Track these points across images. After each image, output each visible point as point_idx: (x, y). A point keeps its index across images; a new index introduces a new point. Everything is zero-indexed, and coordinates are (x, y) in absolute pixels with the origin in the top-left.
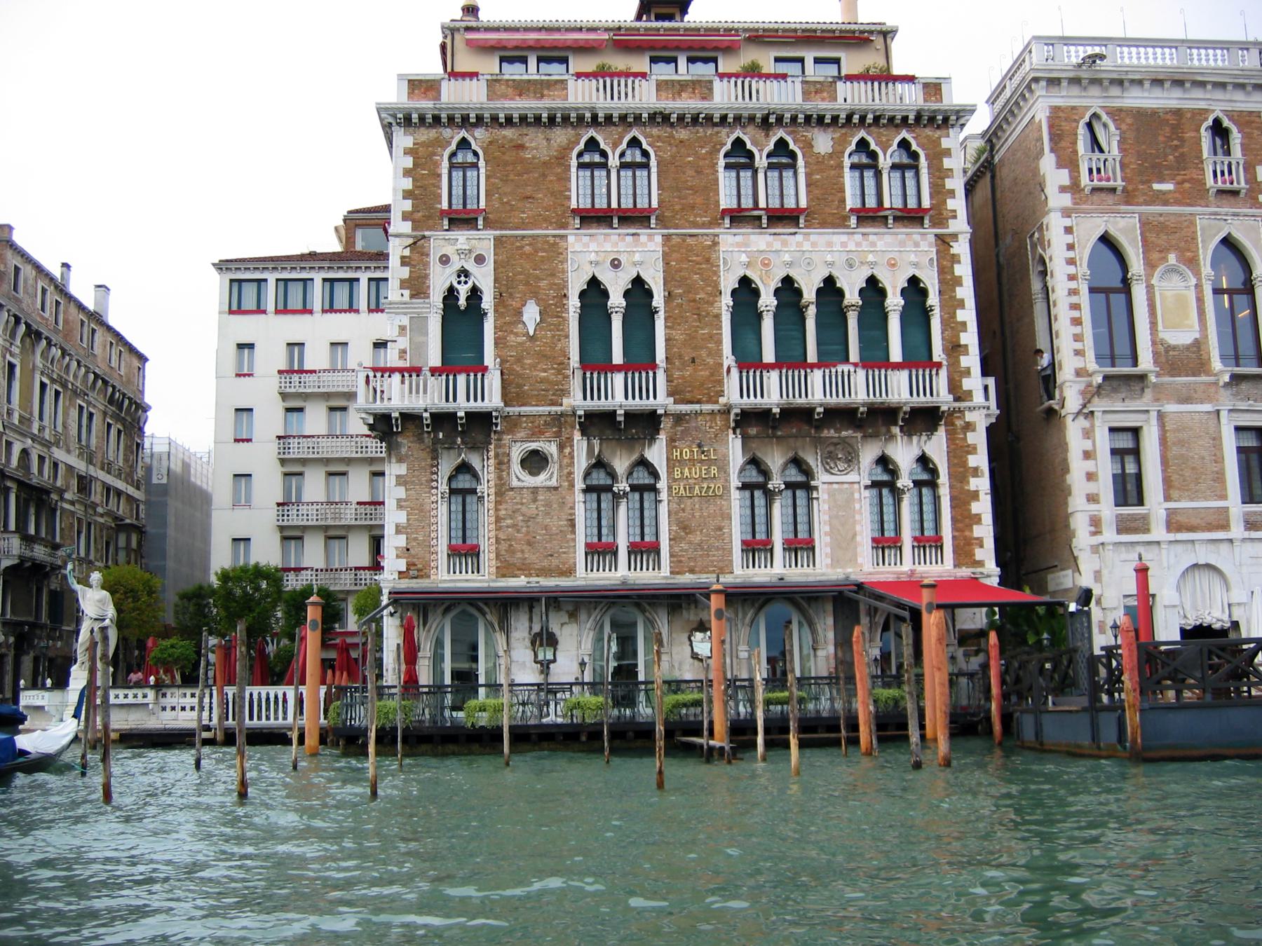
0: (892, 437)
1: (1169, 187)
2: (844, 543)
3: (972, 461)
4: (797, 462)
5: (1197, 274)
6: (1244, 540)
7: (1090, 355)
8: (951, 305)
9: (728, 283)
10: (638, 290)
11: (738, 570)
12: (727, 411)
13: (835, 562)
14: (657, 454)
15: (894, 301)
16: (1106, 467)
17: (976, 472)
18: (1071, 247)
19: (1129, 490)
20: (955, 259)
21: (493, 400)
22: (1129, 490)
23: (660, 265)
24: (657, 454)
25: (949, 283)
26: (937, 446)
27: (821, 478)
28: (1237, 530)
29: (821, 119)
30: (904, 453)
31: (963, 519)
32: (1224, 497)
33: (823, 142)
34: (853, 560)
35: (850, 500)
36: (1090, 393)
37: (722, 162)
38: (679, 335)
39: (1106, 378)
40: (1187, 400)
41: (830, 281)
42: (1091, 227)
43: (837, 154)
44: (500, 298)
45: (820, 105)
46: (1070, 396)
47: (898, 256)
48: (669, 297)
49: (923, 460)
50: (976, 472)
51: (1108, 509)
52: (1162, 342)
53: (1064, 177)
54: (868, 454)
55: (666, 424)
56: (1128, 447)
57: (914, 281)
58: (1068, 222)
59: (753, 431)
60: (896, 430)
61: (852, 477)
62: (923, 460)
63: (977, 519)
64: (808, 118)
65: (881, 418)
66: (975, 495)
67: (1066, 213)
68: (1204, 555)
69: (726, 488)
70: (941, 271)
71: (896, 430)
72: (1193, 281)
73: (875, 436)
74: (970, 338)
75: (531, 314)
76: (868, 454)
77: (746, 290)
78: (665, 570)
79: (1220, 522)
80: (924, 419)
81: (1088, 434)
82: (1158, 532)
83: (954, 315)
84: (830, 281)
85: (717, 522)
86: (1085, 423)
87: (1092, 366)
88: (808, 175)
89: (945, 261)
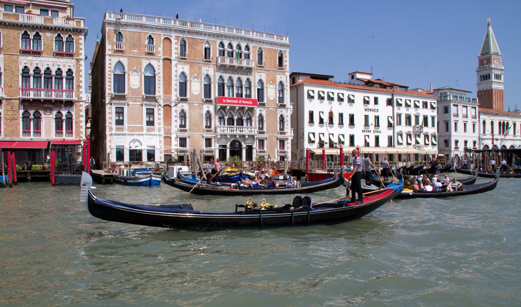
0: (61, 107)
1: (136, 51)
2: (48, 132)
3: (81, 113)
5: (141, 72)
6: (146, 134)
7: (112, 90)
9: (21, 67)
11: (21, 137)
12: (19, 99)
13: (46, 136)
17: (82, 116)
18: (110, 64)
19: (120, 122)
20: (81, 65)
22: (120, 122)
23: (3, 62)
25: (79, 71)
27: (43, 116)
28: (145, 132)
29: (48, 28)
32: (142, 124)
33: (48, 34)
34: (50, 136)
35: (50, 122)
36: (112, 99)
37: (21, 36)
38: (8, 80)
39: (115, 96)
40: (136, 101)
41: (48, 69)
42: (115, 60)
43: (52, 37)
45: (49, 24)
47: (65, 64)
48: (5, 70)
50: (82, 116)
51: (114, 126)
52: (131, 88)
55: (4, 101)
56: (120, 112)
57: (70, 70)
58: (110, 58)
59: (26, 104)
60: (63, 105)
61: (51, 116)
63: (81, 127)
64: (44, 28)
66: (81, 122)
67: (110, 55)
68: (136, 137)
69: (19, 117)
70: (77, 68)
71: (63, 105)
72: (140, 74)
73: (57, 107)
78: (3, 136)
79: (142, 129)
80: (70, 104)
81: (110, 108)
83: (79, 79)
84: (48, 69)
85: (16, 125)
86: (110, 106)
87: (113, 93)
88: (44, 42)
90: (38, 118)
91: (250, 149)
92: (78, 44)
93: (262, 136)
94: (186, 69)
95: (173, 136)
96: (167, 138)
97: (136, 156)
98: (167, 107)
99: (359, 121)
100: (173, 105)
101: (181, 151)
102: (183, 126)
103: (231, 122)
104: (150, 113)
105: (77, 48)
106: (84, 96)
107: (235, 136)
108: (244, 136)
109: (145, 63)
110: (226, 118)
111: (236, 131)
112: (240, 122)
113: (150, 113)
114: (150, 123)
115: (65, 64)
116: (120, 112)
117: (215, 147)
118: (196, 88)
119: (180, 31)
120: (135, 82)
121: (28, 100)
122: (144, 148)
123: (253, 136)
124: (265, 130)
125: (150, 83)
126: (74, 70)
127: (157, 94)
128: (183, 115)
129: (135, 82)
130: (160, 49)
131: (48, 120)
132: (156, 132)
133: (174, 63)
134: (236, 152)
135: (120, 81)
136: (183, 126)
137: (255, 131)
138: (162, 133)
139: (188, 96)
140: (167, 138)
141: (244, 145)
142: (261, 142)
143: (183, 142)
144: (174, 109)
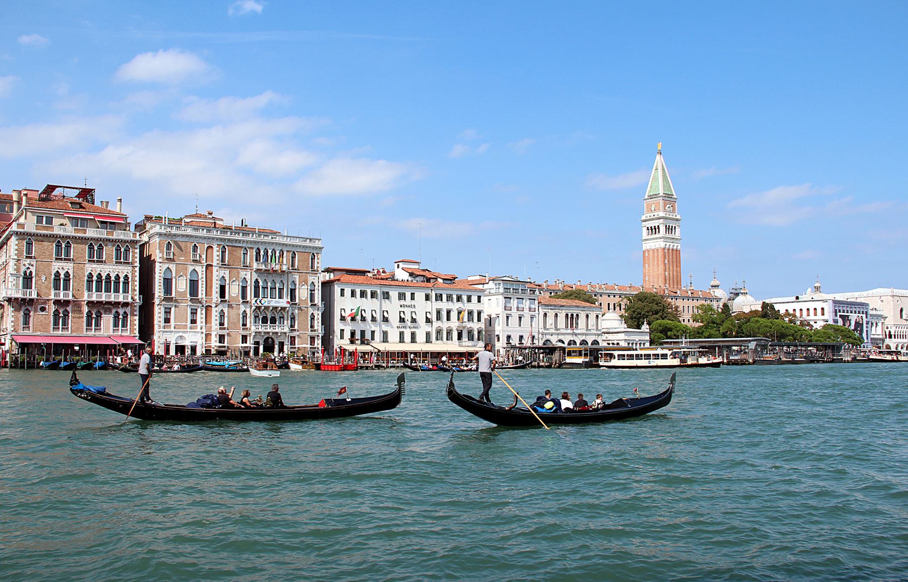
2: (107, 328)
4: (99, 312)
8: (133, 281)
10: (67, 274)
14: (69, 309)
15: (122, 280)
16: (163, 316)
19: (167, 320)
21: (34, 296)
22: (167, 320)
24: (69, 309)
26: (128, 310)
30: (121, 311)
31: (132, 325)
38: (75, 284)
42: (165, 266)
44: (36, 274)
46: (157, 301)
47: (123, 270)
49: (125, 313)
51: (162, 324)
53: (161, 255)
54: (114, 311)
56: (168, 312)
62: (125, 313)
65: (117, 304)
74: (137, 288)
75: (43, 278)
76: (114, 311)
77: (90, 276)
80: (126, 304)
82: (172, 329)
89: (133, 272)
90: (99, 316)
91: (282, 345)
92: (134, 253)
93: (293, 334)
94: (226, 273)
95: (213, 334)
96: (208, 336)
97: (180, 349)
98: (208, 308)
99: (394, 319)
100: (214, 305)
101: (220, 347)
102: (222, 324)
103: (265, 320)
104: (194, 312)
105: (133, 256)
106: (134, 295)
107: (268, 333)
108: (277, 333)
109: (190, 268)
110: (261, 317)
111: (269, 328)
112: (273, 321)
113: (194, 312)
114: (194, 321)
115: (123, 270)
116: (168, 312)
117: (250, 343)
118: (233, 291)
119: (221, 240)
120: (181, 286)
121: (92, 302)
122: (187, 343)
123: (285, 333)
124: (296, 327)
125: (194, 285)
126: (130, 276)
127: (200, 296)
128: (222, 315)
129: (181, 286)
130: (204, 256)
131: (107, 319)
132: (199, 329)
133: (215, 269)
134: (269, 348)
135: (168, 283)
136: (222, 324)
137: (286, 330)
138: (204, 330)
139: (227, 298)
140: (208, 336)
141: (277, 342)
142: (293, 340)
143: (221, 338)
144: (214, 310)
